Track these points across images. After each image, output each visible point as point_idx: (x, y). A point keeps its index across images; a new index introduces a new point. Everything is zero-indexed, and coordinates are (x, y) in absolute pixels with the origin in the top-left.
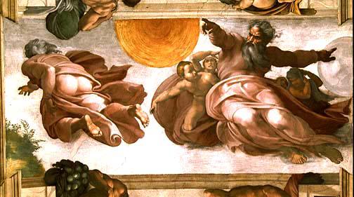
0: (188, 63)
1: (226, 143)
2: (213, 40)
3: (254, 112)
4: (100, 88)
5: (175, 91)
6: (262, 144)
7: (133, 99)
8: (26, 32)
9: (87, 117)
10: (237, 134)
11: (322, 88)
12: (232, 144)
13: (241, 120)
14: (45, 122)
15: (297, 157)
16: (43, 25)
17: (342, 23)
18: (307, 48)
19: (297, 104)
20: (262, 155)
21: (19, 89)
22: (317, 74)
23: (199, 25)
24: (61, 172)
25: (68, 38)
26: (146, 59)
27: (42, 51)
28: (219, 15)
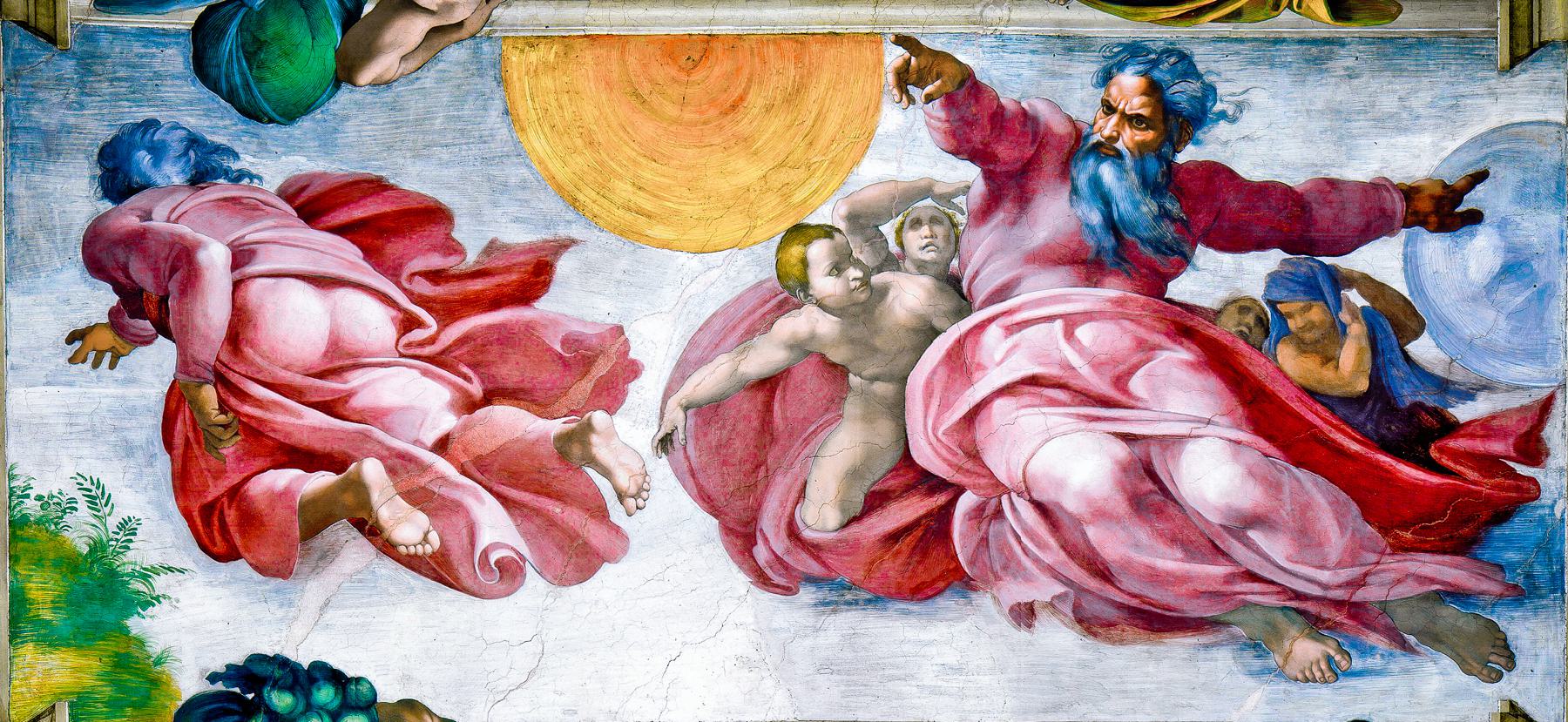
0: (828, 232)
3: (1120, 450)
4: (432, 340)
5: (765, 356)
6: (1155, 594)
7: (587, 385)
8: (105, 87)
9: (372, 470)
10: (1041, 545)
11: (1423, 349)
13: (1060, 484)
14: (183, 483)
15: (1307, 650)
16: (176, 59)
17: (1515, 60)
18: (1359, 171)
19: (1311, 417)
21: (71, 339)
22: (1399, 285)
23: (880, 62)
24: (251, 709)
25: (290, 114)
26: (640, 212)
27: (173, 173)
28: (970, 21)
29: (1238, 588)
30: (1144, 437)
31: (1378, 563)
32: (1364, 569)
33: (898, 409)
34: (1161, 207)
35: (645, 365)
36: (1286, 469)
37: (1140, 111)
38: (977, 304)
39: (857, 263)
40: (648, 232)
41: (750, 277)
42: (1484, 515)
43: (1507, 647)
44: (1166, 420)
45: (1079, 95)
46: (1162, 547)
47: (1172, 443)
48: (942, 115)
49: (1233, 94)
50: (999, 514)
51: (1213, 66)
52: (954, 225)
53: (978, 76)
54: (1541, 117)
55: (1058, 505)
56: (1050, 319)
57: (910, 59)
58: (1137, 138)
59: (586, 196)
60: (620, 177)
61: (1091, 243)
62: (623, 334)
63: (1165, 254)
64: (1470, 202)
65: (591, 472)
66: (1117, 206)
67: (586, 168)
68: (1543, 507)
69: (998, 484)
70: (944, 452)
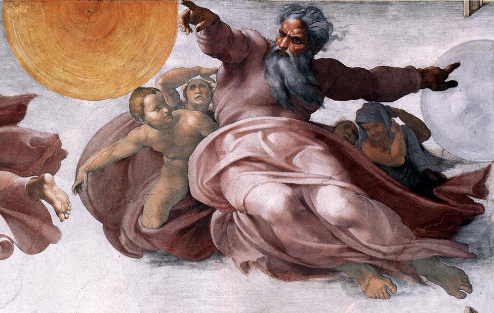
0: (153, 91)
1: (230, 253)
2: (206, 45)
3: (288, 191)
5: (124, 148)
10: (251, 234)
11: (429, 144)
12: (242, 257)
13: (261, 207)
15: (377, 284)
17: (472, 12)
18: (400, 62)
19: (378, 176)
20: (301, 279)
23: (176, 12)
26: (66, 82)
29: (344, 255)
30: (300, 185)
31: (409, 243)
32: (403, 246)
33: (184, 172)
34: (307, 79)
35: (69, 152)
36: (366, 200)
37: (297, 35)
38: (222, 123)
39: (166, 106)
40: (70, 91)
41: (118, 112)
42: (459, 221)
43: (468, 282)
44: (310, 177)
45: (269, 28)
46: (308, 236)
47: (313, 188)
48: (204, 37)
49: (341, 28)
50: (231, 220)
51: (331, 14)
52: (211, 88)
53: (221, 19)
54: (485, 38)
55: (260, 217)
56: (256, 131)
57: (190, 11)
58: (296, 48)
59: (42, 74)
60: (57, 66)
61: (275, 95)
62: (59, 138)
63: (309, 101)
64: (452, 77)
65: (44, 202)
66: (287, 78)
67: (41, 62)
68: (486, 217)
69: (231, 207)
70: (205, 191)
